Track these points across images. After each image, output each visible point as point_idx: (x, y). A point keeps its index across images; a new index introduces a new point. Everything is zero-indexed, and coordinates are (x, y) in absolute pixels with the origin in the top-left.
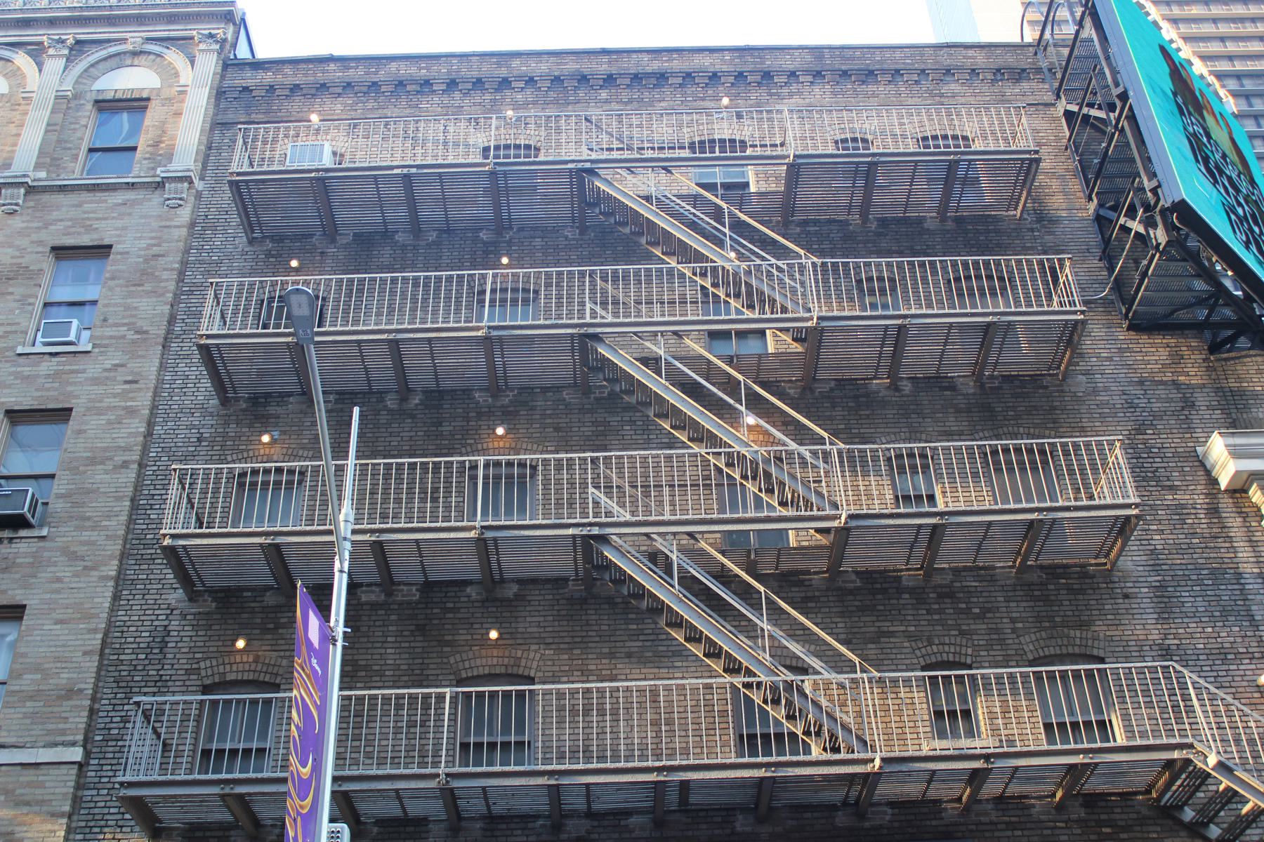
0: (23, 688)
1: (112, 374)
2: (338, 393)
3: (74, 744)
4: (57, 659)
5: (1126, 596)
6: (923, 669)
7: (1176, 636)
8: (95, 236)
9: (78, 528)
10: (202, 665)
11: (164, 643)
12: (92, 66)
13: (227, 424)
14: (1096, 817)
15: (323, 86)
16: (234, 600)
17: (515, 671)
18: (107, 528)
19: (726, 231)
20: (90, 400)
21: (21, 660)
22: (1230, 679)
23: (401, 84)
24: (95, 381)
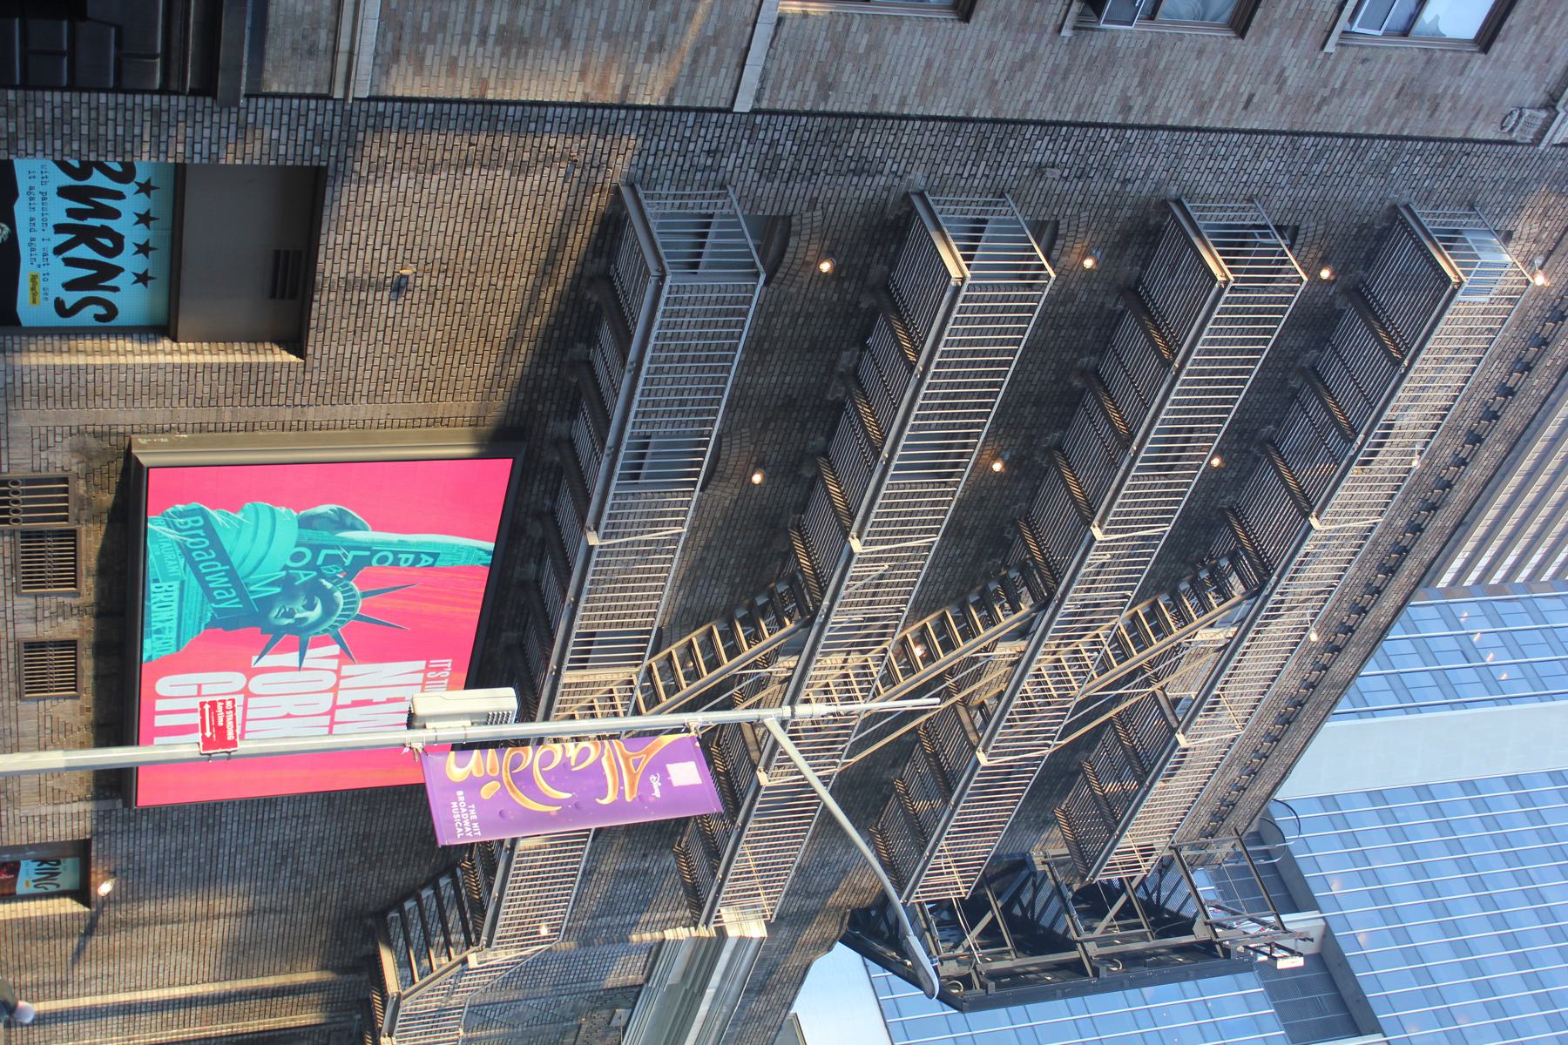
0: (851, 36)
1: (1272, 79)
3: (758, 99)
4: (878, 67)
8: (1514, 31)
9: (1053, 72)
10: (818, 213)
11: (857, 172)
16: (890, 236)
18: (1043, 98)
21: (891, 28)
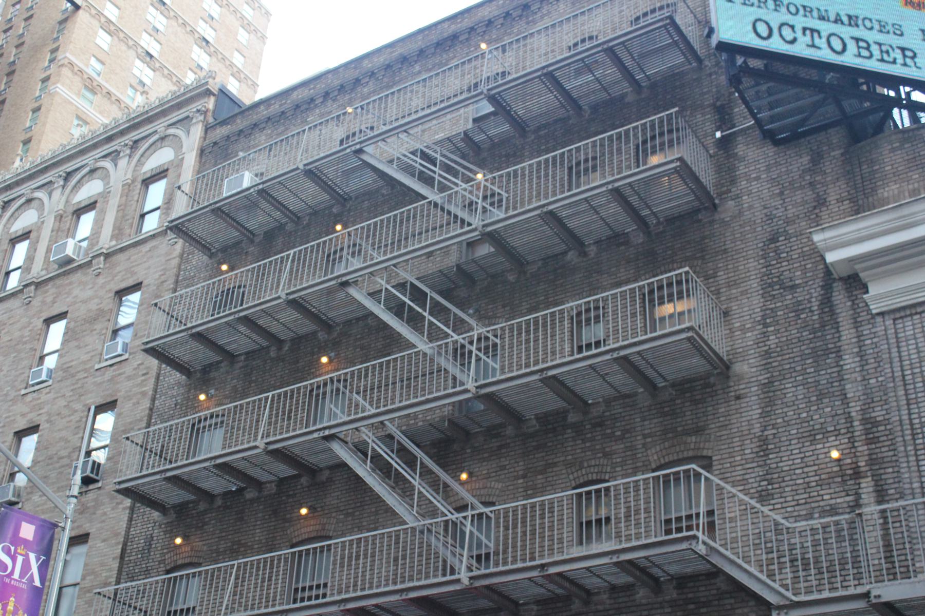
2: (247, 353)
5: (738, 398)
6: (574, 488)
7: (774, 426)
8: (135, 278)
12: (142, 156)
13: (190, 390)
14: (684, 597)
15: (255, 125)
17: (323, 533)
19: (436, 170)
20: (126, 392)
22: (814, 458)
23: (298, 106)
24: (129, 378)
